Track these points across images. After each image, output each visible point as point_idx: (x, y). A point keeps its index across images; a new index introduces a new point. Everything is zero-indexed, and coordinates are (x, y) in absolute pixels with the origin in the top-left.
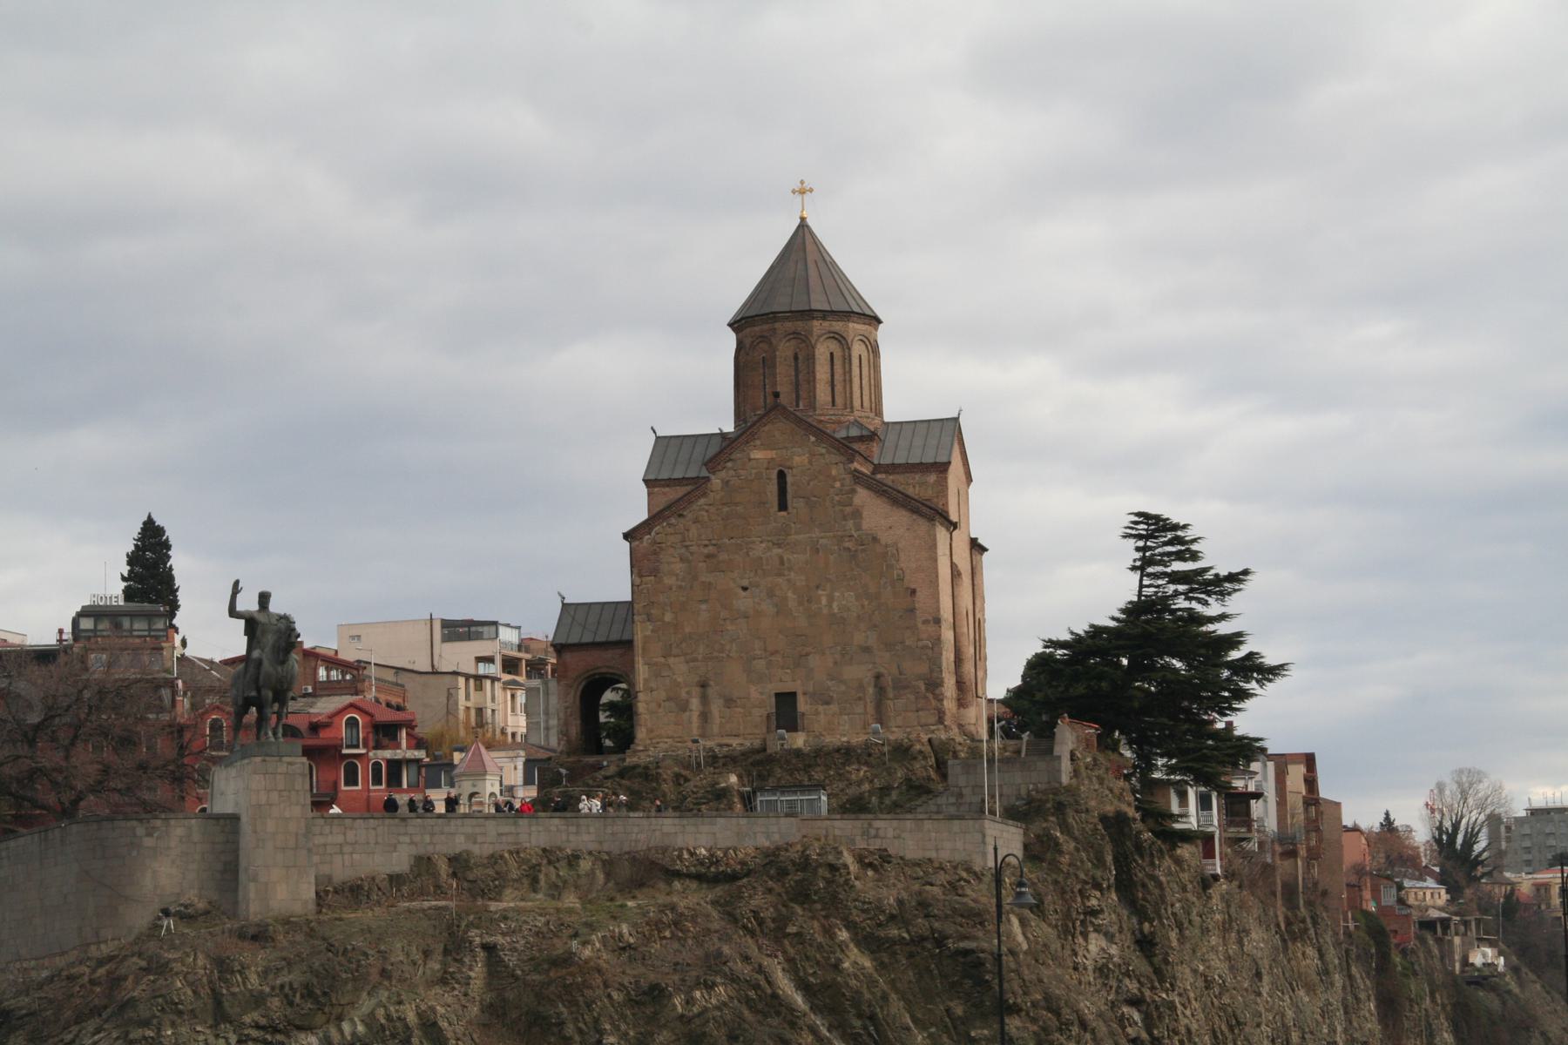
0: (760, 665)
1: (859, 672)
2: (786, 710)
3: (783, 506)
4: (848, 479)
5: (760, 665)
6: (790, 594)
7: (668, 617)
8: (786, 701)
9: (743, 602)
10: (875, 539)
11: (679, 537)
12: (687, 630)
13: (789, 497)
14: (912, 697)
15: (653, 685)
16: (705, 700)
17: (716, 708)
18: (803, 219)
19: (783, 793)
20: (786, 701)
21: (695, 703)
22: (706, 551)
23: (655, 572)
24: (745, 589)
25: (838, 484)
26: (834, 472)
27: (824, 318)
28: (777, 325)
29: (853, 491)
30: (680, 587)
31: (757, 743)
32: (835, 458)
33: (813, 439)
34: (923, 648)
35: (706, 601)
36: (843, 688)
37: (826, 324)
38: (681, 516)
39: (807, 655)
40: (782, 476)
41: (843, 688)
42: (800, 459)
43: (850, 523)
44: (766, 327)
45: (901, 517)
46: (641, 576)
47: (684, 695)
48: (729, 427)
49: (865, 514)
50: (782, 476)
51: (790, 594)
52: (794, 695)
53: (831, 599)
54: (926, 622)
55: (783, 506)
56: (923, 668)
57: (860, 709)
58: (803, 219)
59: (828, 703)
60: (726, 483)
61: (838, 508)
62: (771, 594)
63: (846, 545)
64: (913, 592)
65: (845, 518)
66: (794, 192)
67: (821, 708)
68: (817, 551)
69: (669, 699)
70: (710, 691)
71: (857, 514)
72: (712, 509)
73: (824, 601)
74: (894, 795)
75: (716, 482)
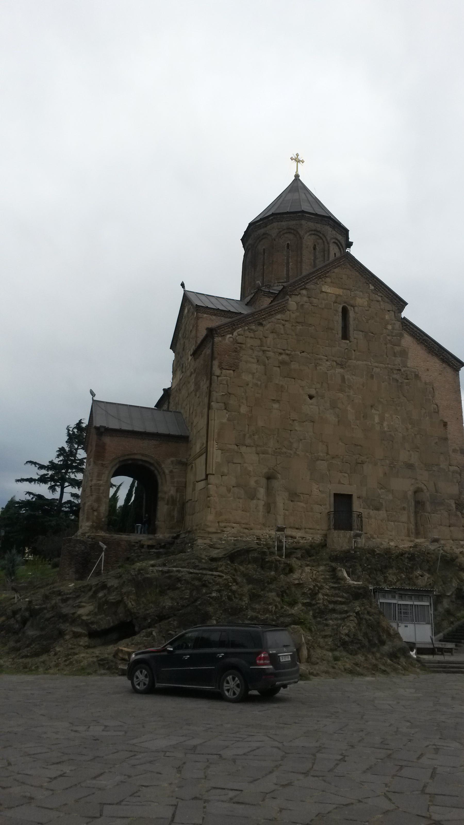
0: (322, 466)
1: (403, 485)
2: (343, 510)
3: (345, 336)
4: (398, 324)
5: (322, 466)
6: (349, 408)
7: (244, 409)
8: (343, 501)
9: (310, 408)
10: (417, 376)
11: (258, 342)
12: (261, 423)
13: (351, 328)
14: (446, 514)
15: (226, 471)
16: (269, 491)
17: (281, 500)
18: (297, 176)
19: (401, 597)
20: (343, 501)
21: (262, 492)
22: (280, 358)
23: (234, 367)
24: (311, 397)
25: (390, 327)
26: (387, 317)
27: (333, 228)
28: (303, 222)
29: (401, 336)
30: (256, 385)
31: (318, 538)
32: (389, 306)
33: (372, 287)
34: (453, 472)
35: (278, 401)
36: (390, 497)
37: (334, 232)
38: (261, 324)
39: (363, 463)
40: (345, 311)
41: (390, 497)
42: (361, 301)
43: (398, 360)
44: (294, 222)
45: (435, 364)
46: (221, 368)
47: (252, 483)
48: (350, 241)
49: (410, 354)
50: (345, 311)
51: (349, 408)
52: (350, 497)
53: (382, 419)
54: (454, 451)
55: (345, 336)
56: (455, 490)
57: (404, 518)
58: (297, 176)
59: (378, 509)
60: (301, 306)
61: (389, 346)
62: (333, 406)
63: (395, 376)
64: (445, 424)
65: (395, 355)
66: (292, 159)
67: (372, 513)
68: (372, 377)
69: (238, 486)
70: (276, 484)
71: (404, 353)
72: (288, 325)
73: (377, 420)
74: (446, 604)
75: (292, 303)
